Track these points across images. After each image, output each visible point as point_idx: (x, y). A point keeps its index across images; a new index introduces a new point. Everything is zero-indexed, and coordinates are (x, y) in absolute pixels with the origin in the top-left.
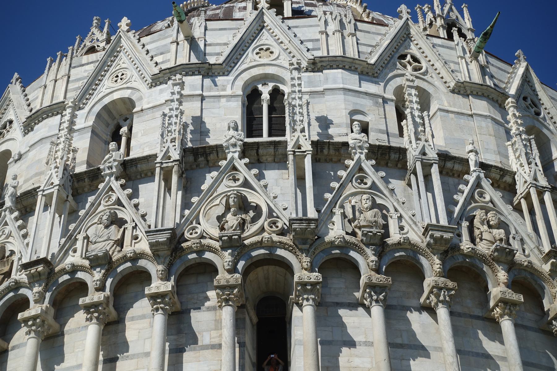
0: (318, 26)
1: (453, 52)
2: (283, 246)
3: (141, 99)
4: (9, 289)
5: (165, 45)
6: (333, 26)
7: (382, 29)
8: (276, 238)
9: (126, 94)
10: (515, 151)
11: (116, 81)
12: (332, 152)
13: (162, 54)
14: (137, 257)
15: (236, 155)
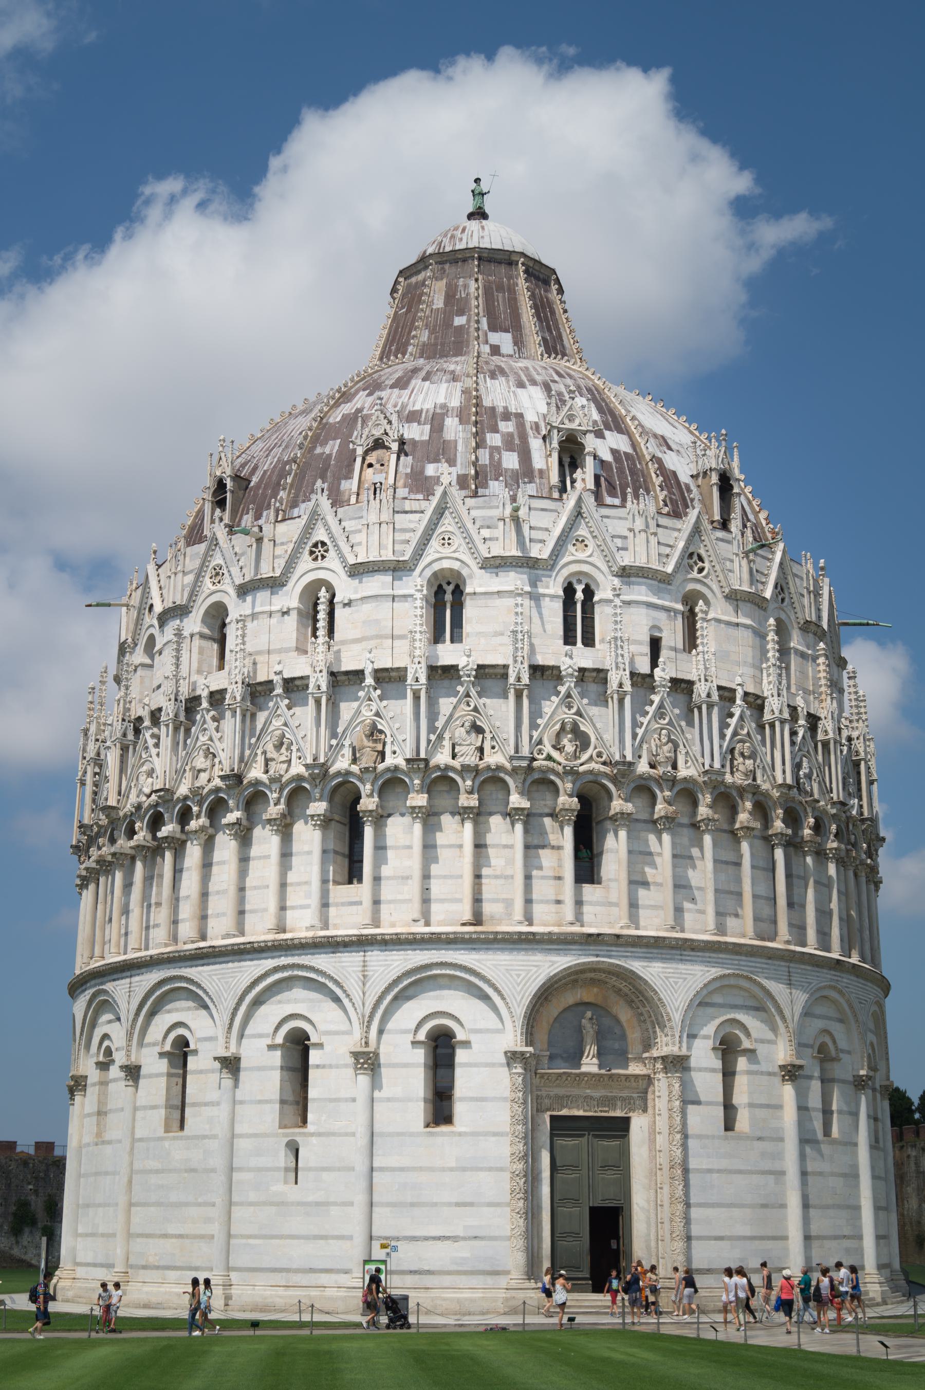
0: (626, 519)
1: (730, 546)
2: (606, 775)
3: (471, 576)
4: (388, 770)
5: (491, 518)
6: (639, 524)
7: (677, 524)
8: (603, 768)
9: (456, 565)
10: (769, 675)
11: (443, 544)
12: (639, 679)
13: (488, 527)
14: (499, 768)
15: (572, 685)
